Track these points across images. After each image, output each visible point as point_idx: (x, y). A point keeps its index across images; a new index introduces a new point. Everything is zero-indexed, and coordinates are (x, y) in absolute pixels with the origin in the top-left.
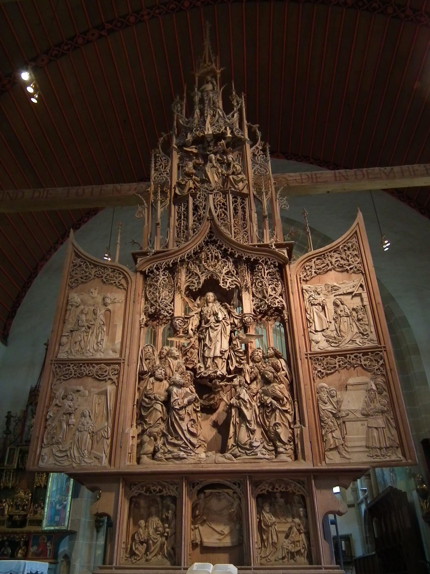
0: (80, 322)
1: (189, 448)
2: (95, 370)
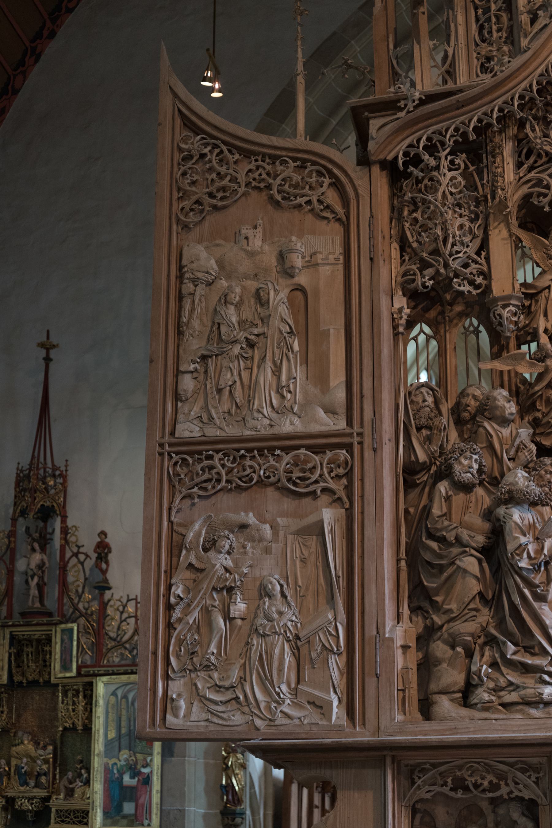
0: (223, 329)
2: (282, 466)
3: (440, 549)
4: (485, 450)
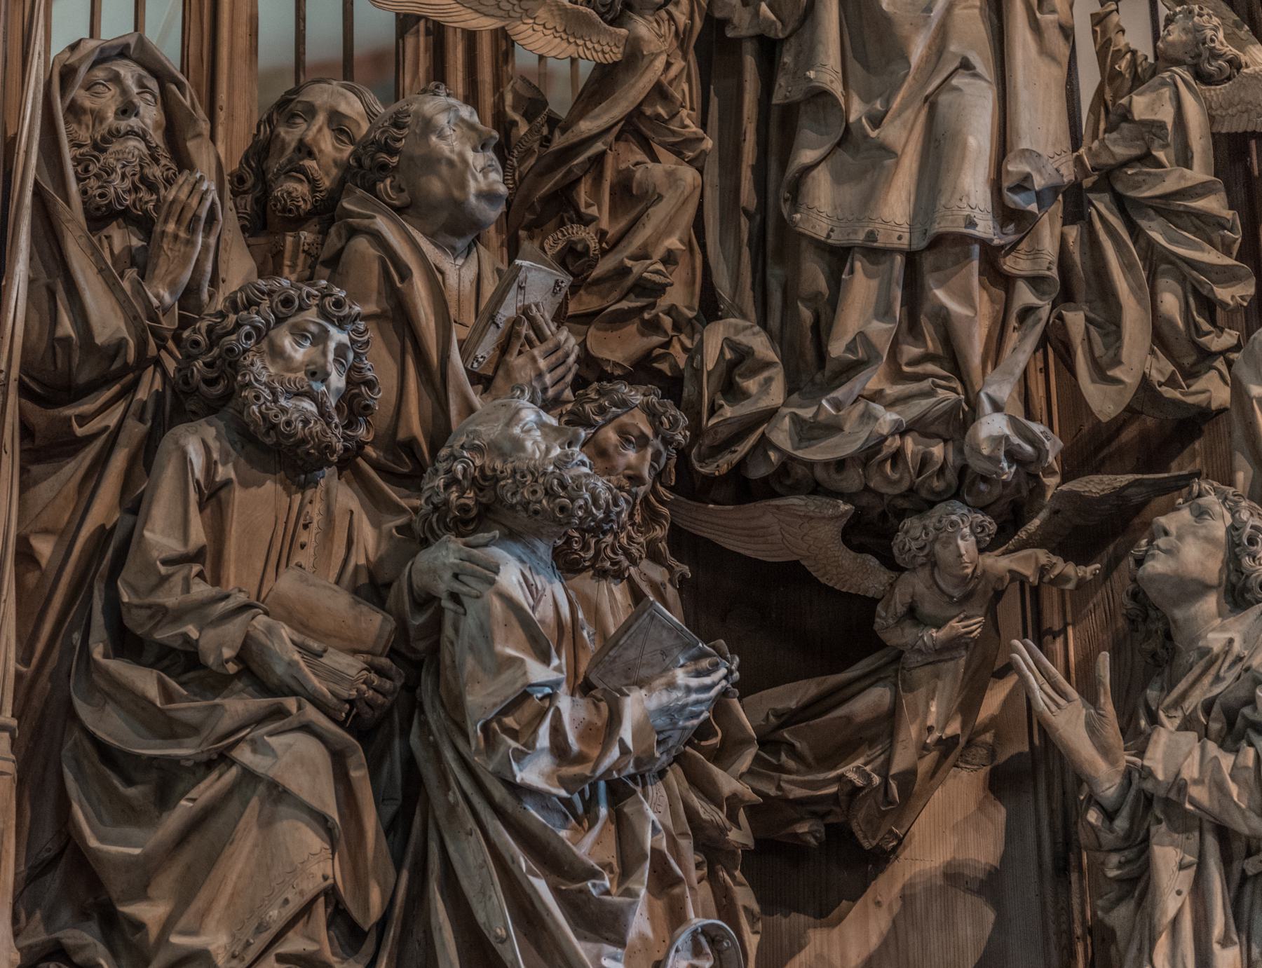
3: (168, 695)
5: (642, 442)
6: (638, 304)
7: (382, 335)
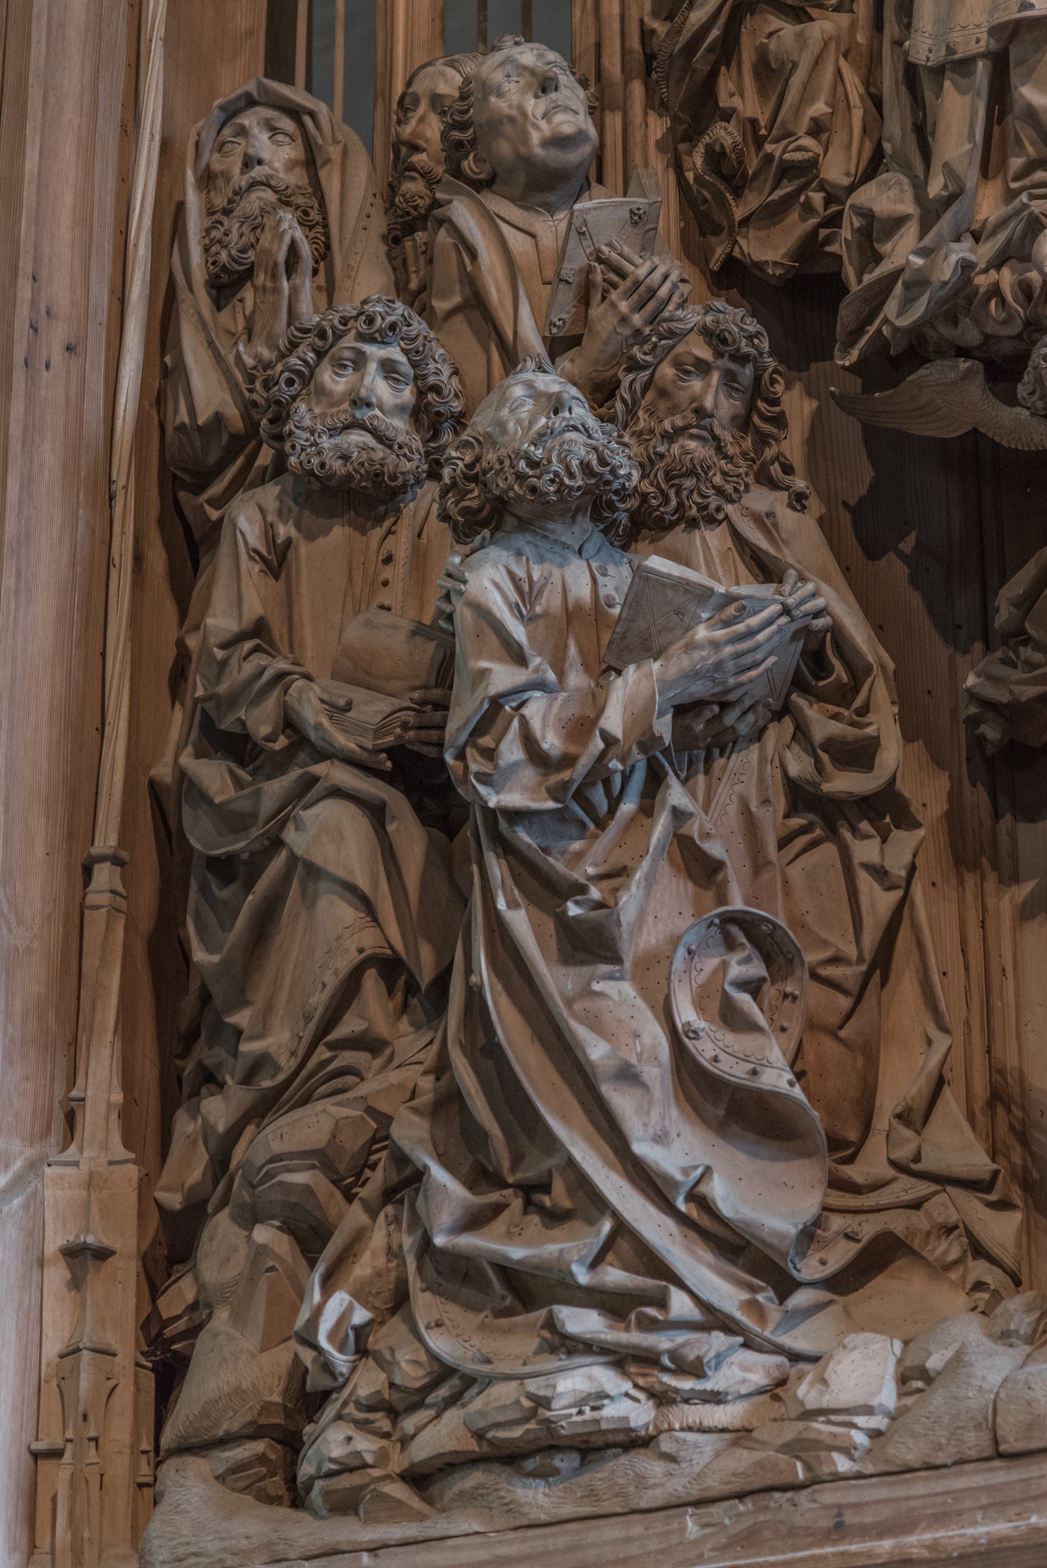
1: (680, 1304)
4: (458, 319)
5: (703, 368)
6: (789, 190)
7: (470, 323)
